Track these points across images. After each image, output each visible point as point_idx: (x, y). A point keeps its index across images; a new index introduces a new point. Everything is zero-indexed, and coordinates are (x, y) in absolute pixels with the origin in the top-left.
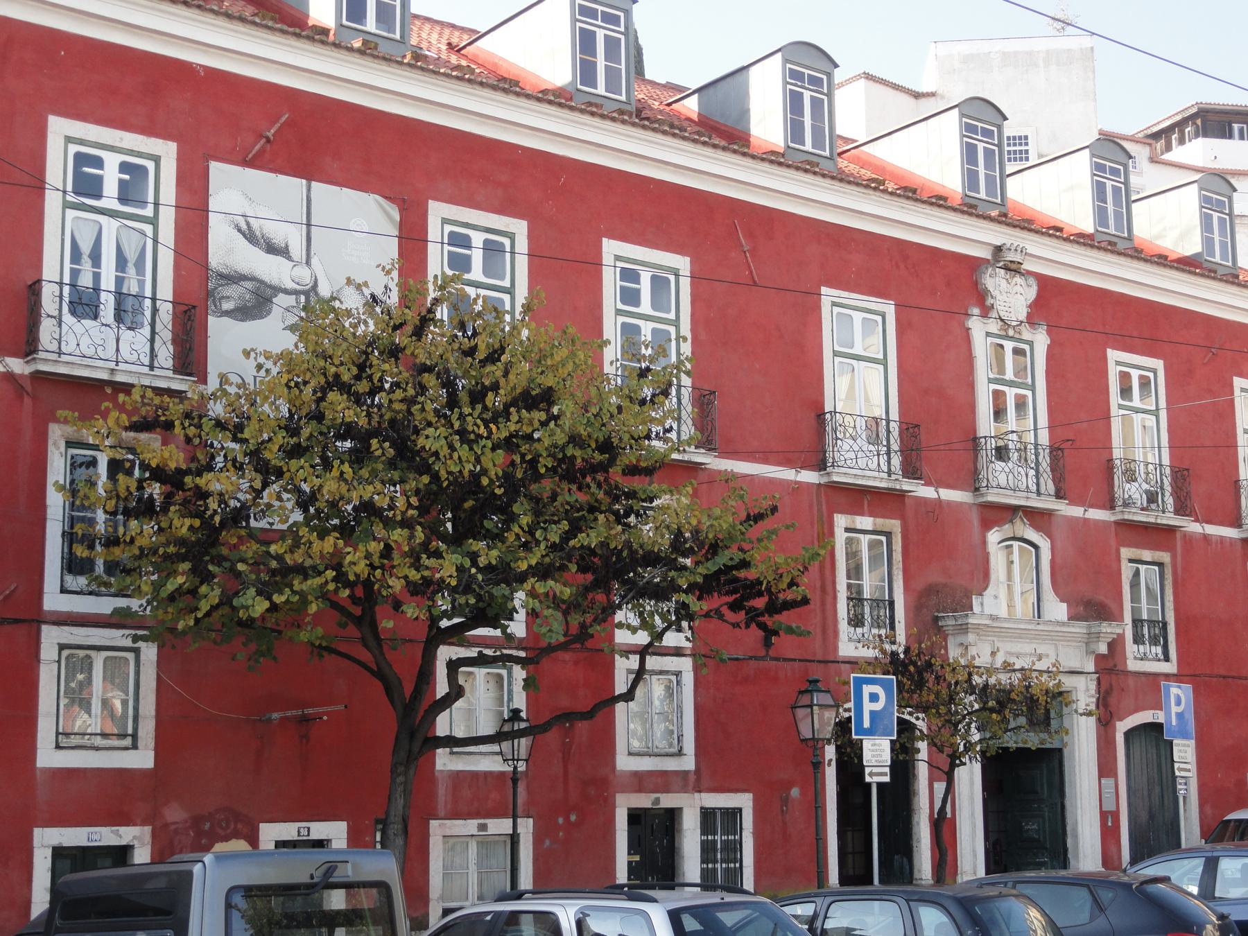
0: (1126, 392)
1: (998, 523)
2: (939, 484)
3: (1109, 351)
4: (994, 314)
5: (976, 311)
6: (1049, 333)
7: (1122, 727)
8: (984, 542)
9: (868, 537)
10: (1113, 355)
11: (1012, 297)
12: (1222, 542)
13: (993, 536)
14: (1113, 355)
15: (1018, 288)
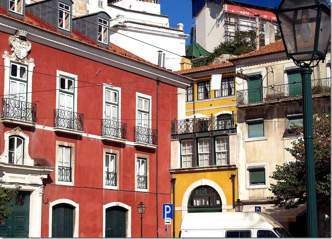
0: (63, 86)
3: (58, 71)
4: (13, 54)
5: (6, 52)
6: (35, 62)
7: (52, 204)
11: (22, 49)
12: (94, 141)
14: (59, 72)
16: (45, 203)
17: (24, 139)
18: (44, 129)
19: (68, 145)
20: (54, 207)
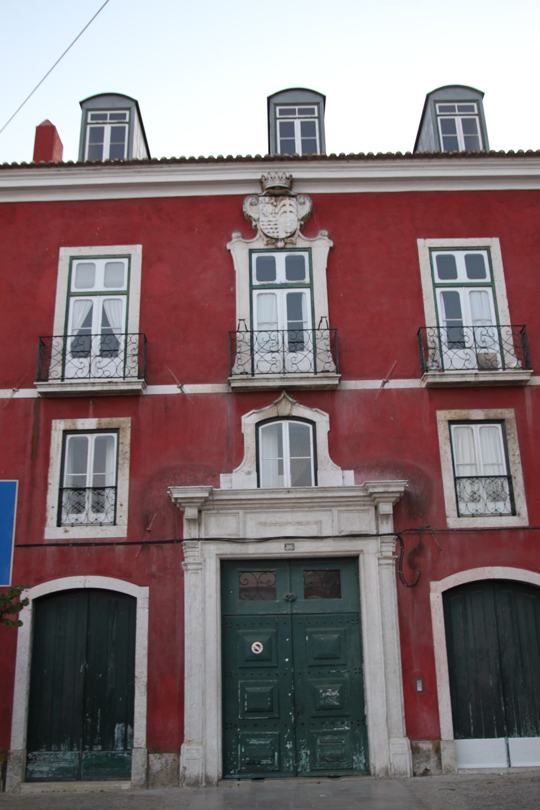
1: (258, 406)
2: (183, 381)
3: (420, 242)
8: (239, 425)
9: (95, 435)
10: (423, 245)
13: (249, 420)
14: (423, 245)
15: (288, 208)
16: (411, 582)
17: (313, 423)
18: (386, 386)
19: (486, 415)
20: (446, 594)
